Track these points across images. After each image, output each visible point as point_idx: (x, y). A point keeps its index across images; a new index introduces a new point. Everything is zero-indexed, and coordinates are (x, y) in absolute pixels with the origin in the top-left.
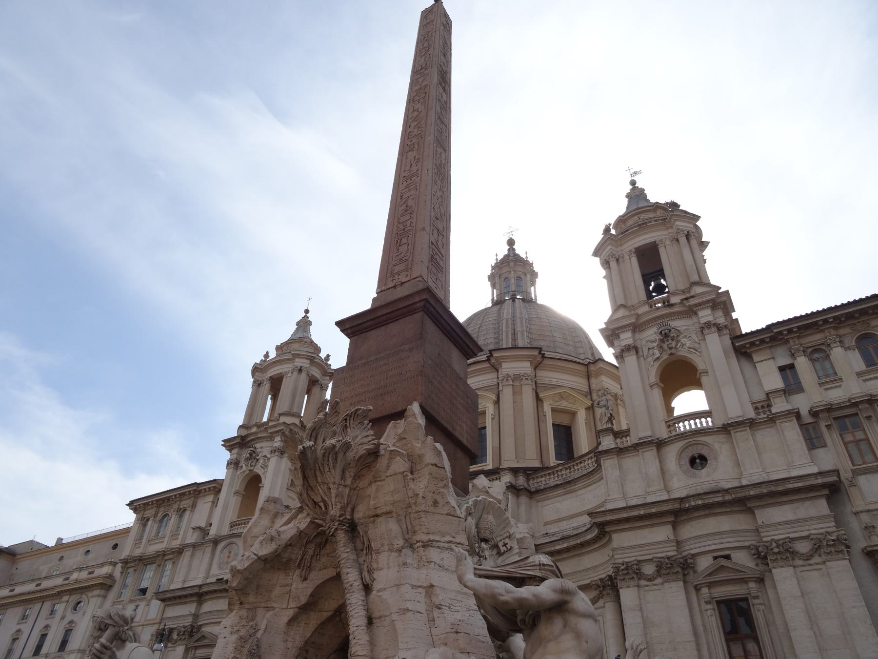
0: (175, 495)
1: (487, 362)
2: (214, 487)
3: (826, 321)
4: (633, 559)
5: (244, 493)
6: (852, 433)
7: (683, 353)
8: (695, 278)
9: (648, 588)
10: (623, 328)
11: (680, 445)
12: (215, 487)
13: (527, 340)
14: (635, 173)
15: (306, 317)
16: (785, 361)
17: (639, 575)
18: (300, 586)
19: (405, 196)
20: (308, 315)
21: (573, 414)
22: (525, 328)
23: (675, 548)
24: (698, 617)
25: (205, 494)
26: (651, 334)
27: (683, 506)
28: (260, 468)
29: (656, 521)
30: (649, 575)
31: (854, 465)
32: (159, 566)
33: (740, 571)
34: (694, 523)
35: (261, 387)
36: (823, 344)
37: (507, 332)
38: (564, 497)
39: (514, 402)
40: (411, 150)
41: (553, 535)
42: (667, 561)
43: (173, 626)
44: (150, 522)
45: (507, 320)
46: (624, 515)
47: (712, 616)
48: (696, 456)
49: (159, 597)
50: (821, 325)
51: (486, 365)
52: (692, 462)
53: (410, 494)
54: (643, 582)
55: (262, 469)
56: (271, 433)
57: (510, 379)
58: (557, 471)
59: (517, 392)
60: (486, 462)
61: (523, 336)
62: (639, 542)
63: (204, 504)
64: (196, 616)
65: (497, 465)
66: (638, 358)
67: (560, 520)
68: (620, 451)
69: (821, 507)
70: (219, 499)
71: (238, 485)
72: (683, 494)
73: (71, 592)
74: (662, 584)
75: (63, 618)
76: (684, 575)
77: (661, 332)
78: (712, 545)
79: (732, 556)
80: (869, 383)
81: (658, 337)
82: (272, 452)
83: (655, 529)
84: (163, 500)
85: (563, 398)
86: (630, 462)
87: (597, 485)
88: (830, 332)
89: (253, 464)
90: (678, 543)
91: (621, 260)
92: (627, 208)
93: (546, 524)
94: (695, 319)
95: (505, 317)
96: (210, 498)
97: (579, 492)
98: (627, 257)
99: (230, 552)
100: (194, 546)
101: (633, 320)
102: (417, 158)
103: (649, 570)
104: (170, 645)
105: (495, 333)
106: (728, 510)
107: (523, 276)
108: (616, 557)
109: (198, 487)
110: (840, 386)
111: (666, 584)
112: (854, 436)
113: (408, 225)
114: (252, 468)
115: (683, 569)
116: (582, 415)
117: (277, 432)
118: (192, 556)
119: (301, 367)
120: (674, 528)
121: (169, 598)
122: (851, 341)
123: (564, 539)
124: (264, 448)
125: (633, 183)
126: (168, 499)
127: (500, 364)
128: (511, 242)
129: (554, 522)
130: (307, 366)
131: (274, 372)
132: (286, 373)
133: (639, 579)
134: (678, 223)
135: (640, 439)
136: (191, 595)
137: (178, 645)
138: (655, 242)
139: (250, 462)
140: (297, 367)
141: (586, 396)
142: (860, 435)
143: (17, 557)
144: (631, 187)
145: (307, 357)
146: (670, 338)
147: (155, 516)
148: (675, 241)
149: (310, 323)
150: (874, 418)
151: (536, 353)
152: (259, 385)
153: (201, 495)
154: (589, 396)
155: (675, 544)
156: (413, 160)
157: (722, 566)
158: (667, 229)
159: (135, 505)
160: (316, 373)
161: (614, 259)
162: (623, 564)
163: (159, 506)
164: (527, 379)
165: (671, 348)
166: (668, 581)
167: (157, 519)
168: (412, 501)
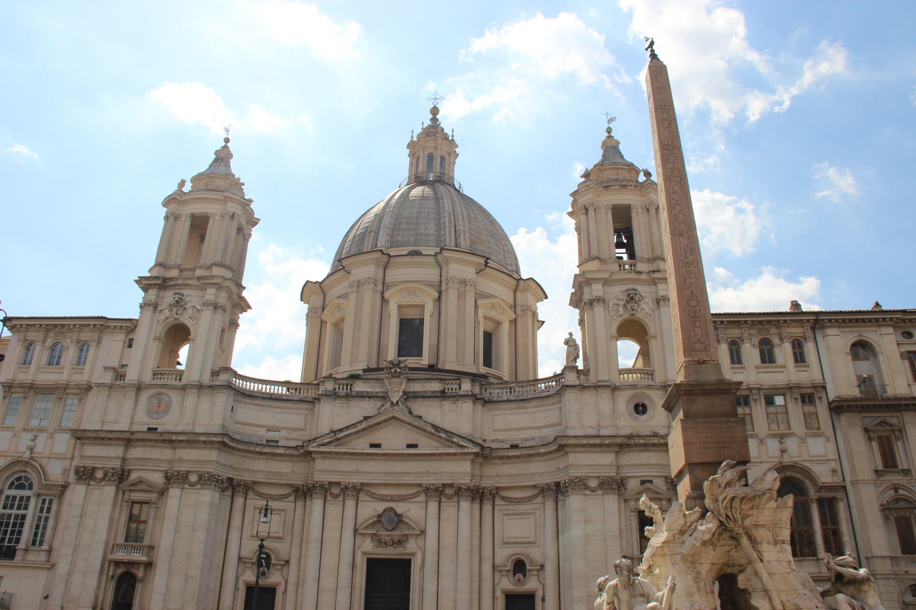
0: (75, 325)
1: (434, 257)
2: (129, 326)
3: (746, 322)
4: (583, 474)
5: (165, 340)
6: (743, 408)
7: (640, 315)
8: (659, 253)
9: (589, 497)
10: (597, 280)
11: (630, 393)
12: (128, 327)
13: (468, 242)
14: (611, 120)
15: (226, 147)
17: (587, 487)
18: (713, 553)
19: (687, 281)
20: (229, 145)
21: (498, 324)
22: (467, 228)
23: (616, 471)
24: (623, 520)
25: (115, 331)
26: (617, 292)
27: (629, 442)
28: (188, 318)
29: (605, 449)
30: (594, 488)
32: (60, 399)
33: (659, 493)
34: (631, 455)
35: (178, 222)
36: (739, 338)
37: (450, 227)
38: (514, 411)
39: (458, 306)
40: (681, 235)
41: (503, 442)
42: (610, 480)
43: (96, 466)
44: (38, 348)
45: (449, 214)
46: (584, 442)
47: (634, 520)
48: (640, 404)
49: (77, 435)
50: (742, 324)
51: (432, 260)
52: (636, 407)
53: (777, 518)
54: (588, 492)
55: (191, 320)
56: (202, 283)
57: (456, 281)
59: (461, 296)
60: (422, 356)
61: (465, 235)
62: (589, 463)
63: (114, 343)
64: (124, 459)
65: (433, 362)
66: (605, 309)
67: (510, 430)
68: (583, 388)
70: (131, 340)
71: (159, 329)
72: (627, 432)
74: (603, 495)
76: (619, 490)
77: (629, 294)
78: (643, 473)
79: (654, 481)
80: (760, 374)
81: (626, 298)
82: (206, 304)
83: (603, 455)
84: (55, 326)
85: (494, 307)
86: (589, 397)
87: (548, 408)
88: (745, 330)
89: (179, 312)
90: (618, 467)
91: (597, 211)
92: (604, 156)
93: (495, 431)
94: (653, 288)
95: (446, 209)
96: (121, 337)
97: (530, 410)
98: (603, 210)
99: (160, 403)
101: (607, 276)
102: (689, 246)
103: (593, 483)
104: (92, 483)
105: (436, 224)
107: (446, 156)
108: (570, 471)
109: (106, 322)
110: (742, 373)
111: (606, 496)
112: (744, 411)
113: (698, 311)
114: (178, 316)
115: (619, 486)
116: (506, 327)
117: (212, 284)
118: (109, 396)
119: (234, 213)
120: (617, 453)
121: (81, 436)
122: (756, 340)
123: (514, 447)
124: (193, 297)
125: (609, 131)
126: (63, 326)
127: (447, 264)
128: (435, 111)
129: (504, 430)
130: (239, 212)
131: (199, 208)
132: (213, 214)
133: (586, 489)
135: (599, 381)
136: (118, 439)
137: (107, 485)
138: (630, 205)
139: (175, 309)
140: (229, 212)
141: (511, 308)
142: (747, 410)
144: (607, 134)
146: (634, 301)
147: (44, 341)
148: (645, 210)
149: (231, 156)
150: (758, 401)
151: (482, 261)
152: (176, 219)
153: (108, 330)
154: (513, 309)
155: (616, 468)
156: (686, 246)
157: (649, 488)
158: (641, 196)
159: (14, 323)
161: (593, 209)
162: (576, 478)
163: (48, 331)
164: (471, 285)
165: (633, 310)
166: (607, 494)
167: (47, 344)
168: (778, 522)
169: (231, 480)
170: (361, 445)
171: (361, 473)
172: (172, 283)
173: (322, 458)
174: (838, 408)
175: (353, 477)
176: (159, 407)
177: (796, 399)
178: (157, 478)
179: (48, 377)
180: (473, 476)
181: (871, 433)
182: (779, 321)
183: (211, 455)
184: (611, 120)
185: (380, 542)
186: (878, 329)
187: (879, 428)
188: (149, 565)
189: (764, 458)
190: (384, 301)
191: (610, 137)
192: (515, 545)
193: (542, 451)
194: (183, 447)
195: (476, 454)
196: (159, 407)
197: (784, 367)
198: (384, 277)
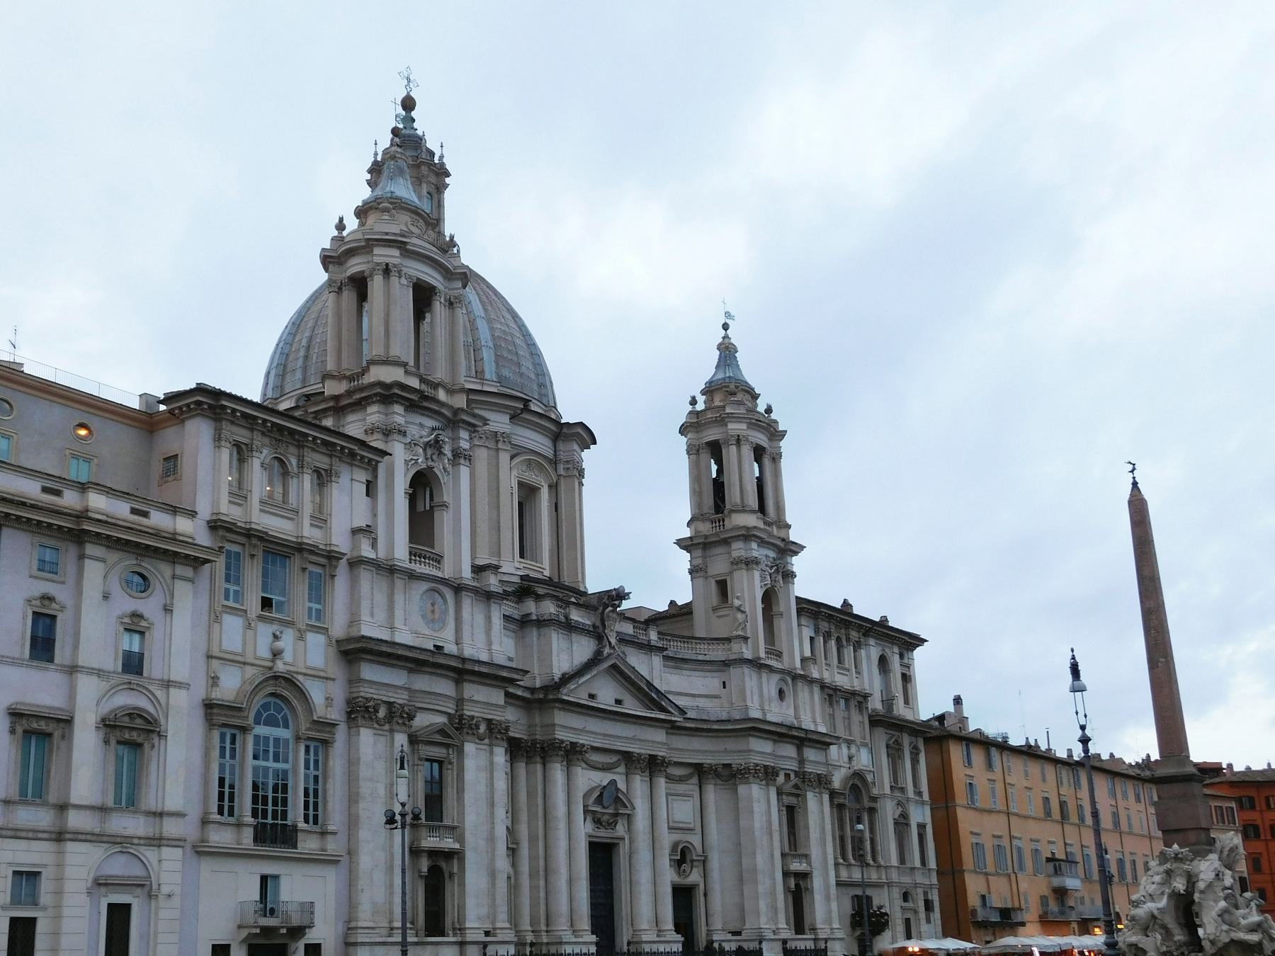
16: (813, 636)
58: (666, 639)
97: (684, 671)
173: (563, 709)
174: (876, 721)
175: (581, 737)
176: (433, 612)
177: (856, 706)
181: (889, 750)
184: (728, 314)
185: (598, 822)
186: (890, 645)
187: (894, 746)
189: (842, 764)
191: (726, 337)
192: (677, 831)
193: (715, 727)
196: (433, 612)
197: (849, 671)
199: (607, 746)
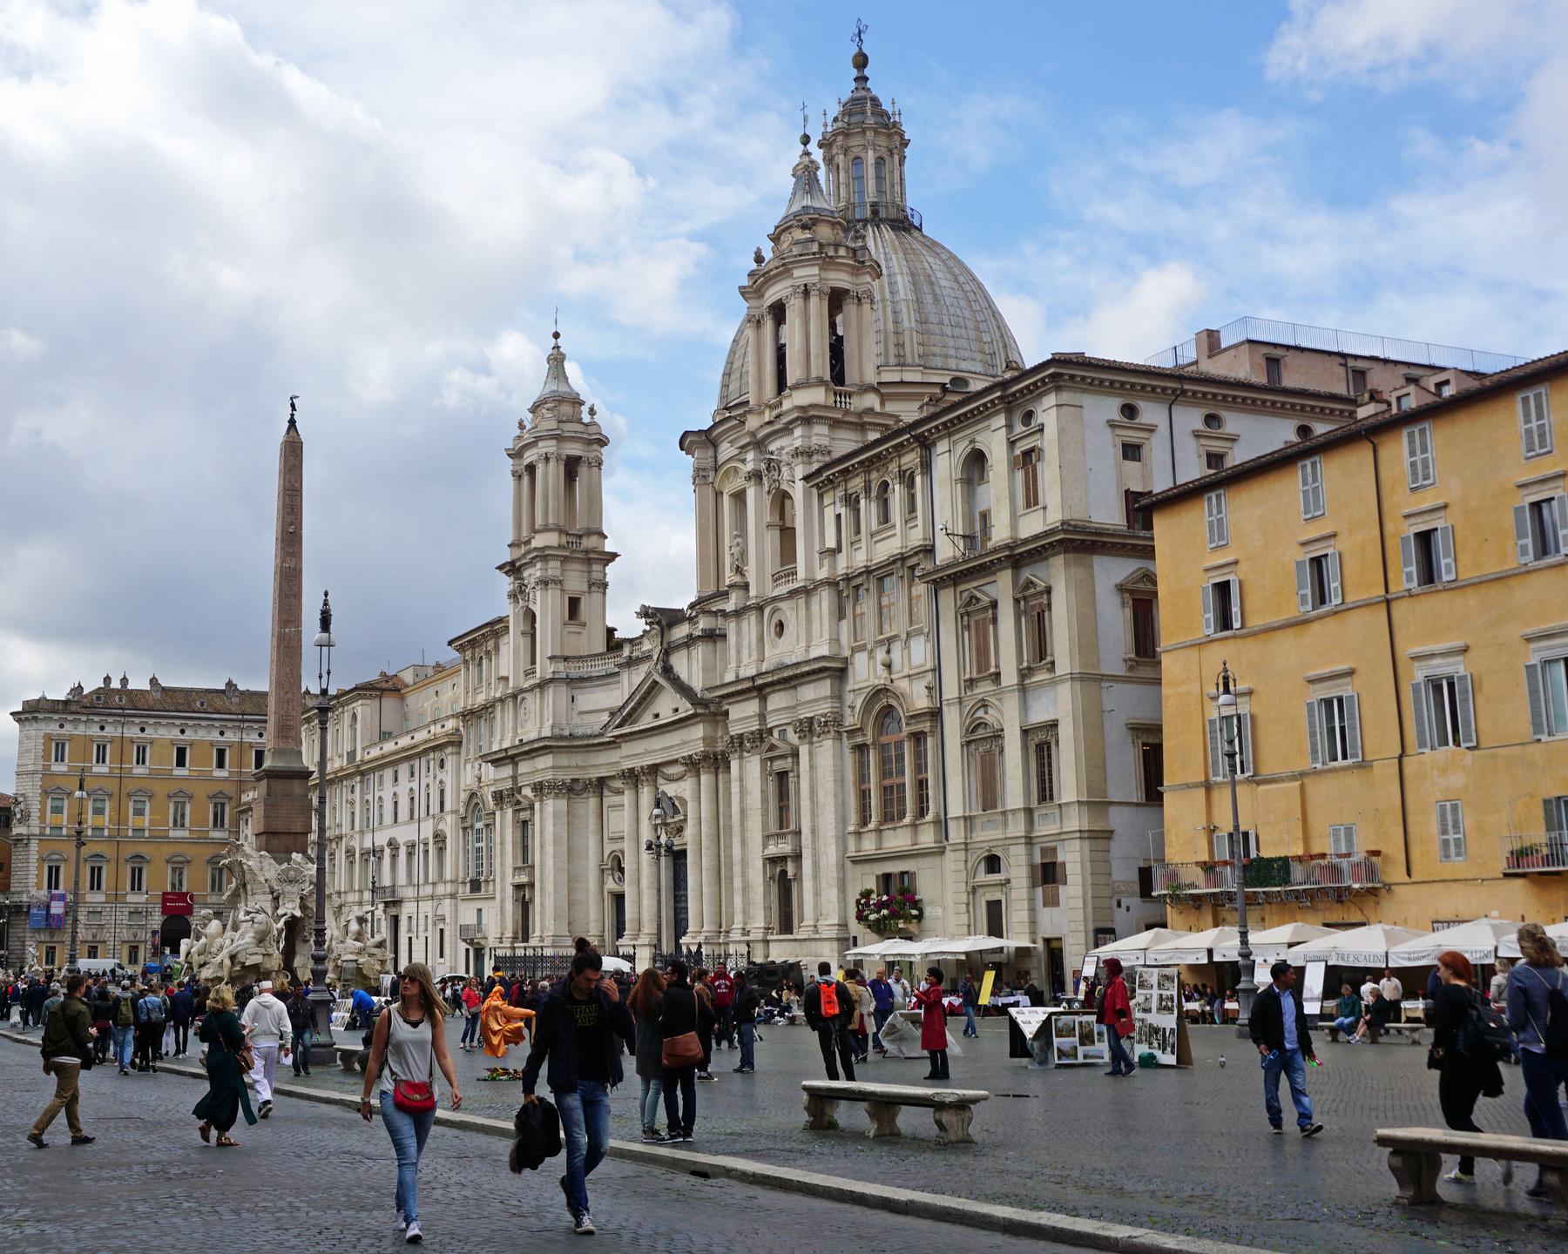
7: (784, 487)
15: (557, 347)
31: (856, 641)
54: (745, 754)
62: (742, 716)
64: (514, 778)
69: (824, 688)
73: (434, 749)
75: (435, 778)
90: (762, 717)
96: (506, 637)
100: (502, 700)
106: (782, 687)
130: (553, 449)
134: (797, 273)
143: (403, 692)
145: (551, 437)
152: (520, 476)
160: (574, 449)
163: (473, 647)
169: (575, 781)
170: (646, 722)
171: (651, 752)
172: (518, 564)
173: (626, 742)
178: (527, 792)
179: (481, 699)
180: (709, 740)
182: (881, 452)
183: (545, 762)
188: (532, 885)
190: (718, 494)
194: (537, 756)
195: (695, 716)
198: (716, 457)
199: (666, 759)
